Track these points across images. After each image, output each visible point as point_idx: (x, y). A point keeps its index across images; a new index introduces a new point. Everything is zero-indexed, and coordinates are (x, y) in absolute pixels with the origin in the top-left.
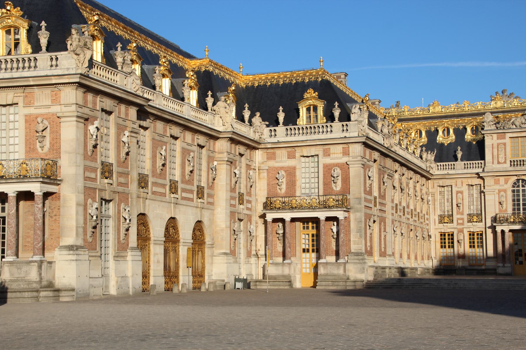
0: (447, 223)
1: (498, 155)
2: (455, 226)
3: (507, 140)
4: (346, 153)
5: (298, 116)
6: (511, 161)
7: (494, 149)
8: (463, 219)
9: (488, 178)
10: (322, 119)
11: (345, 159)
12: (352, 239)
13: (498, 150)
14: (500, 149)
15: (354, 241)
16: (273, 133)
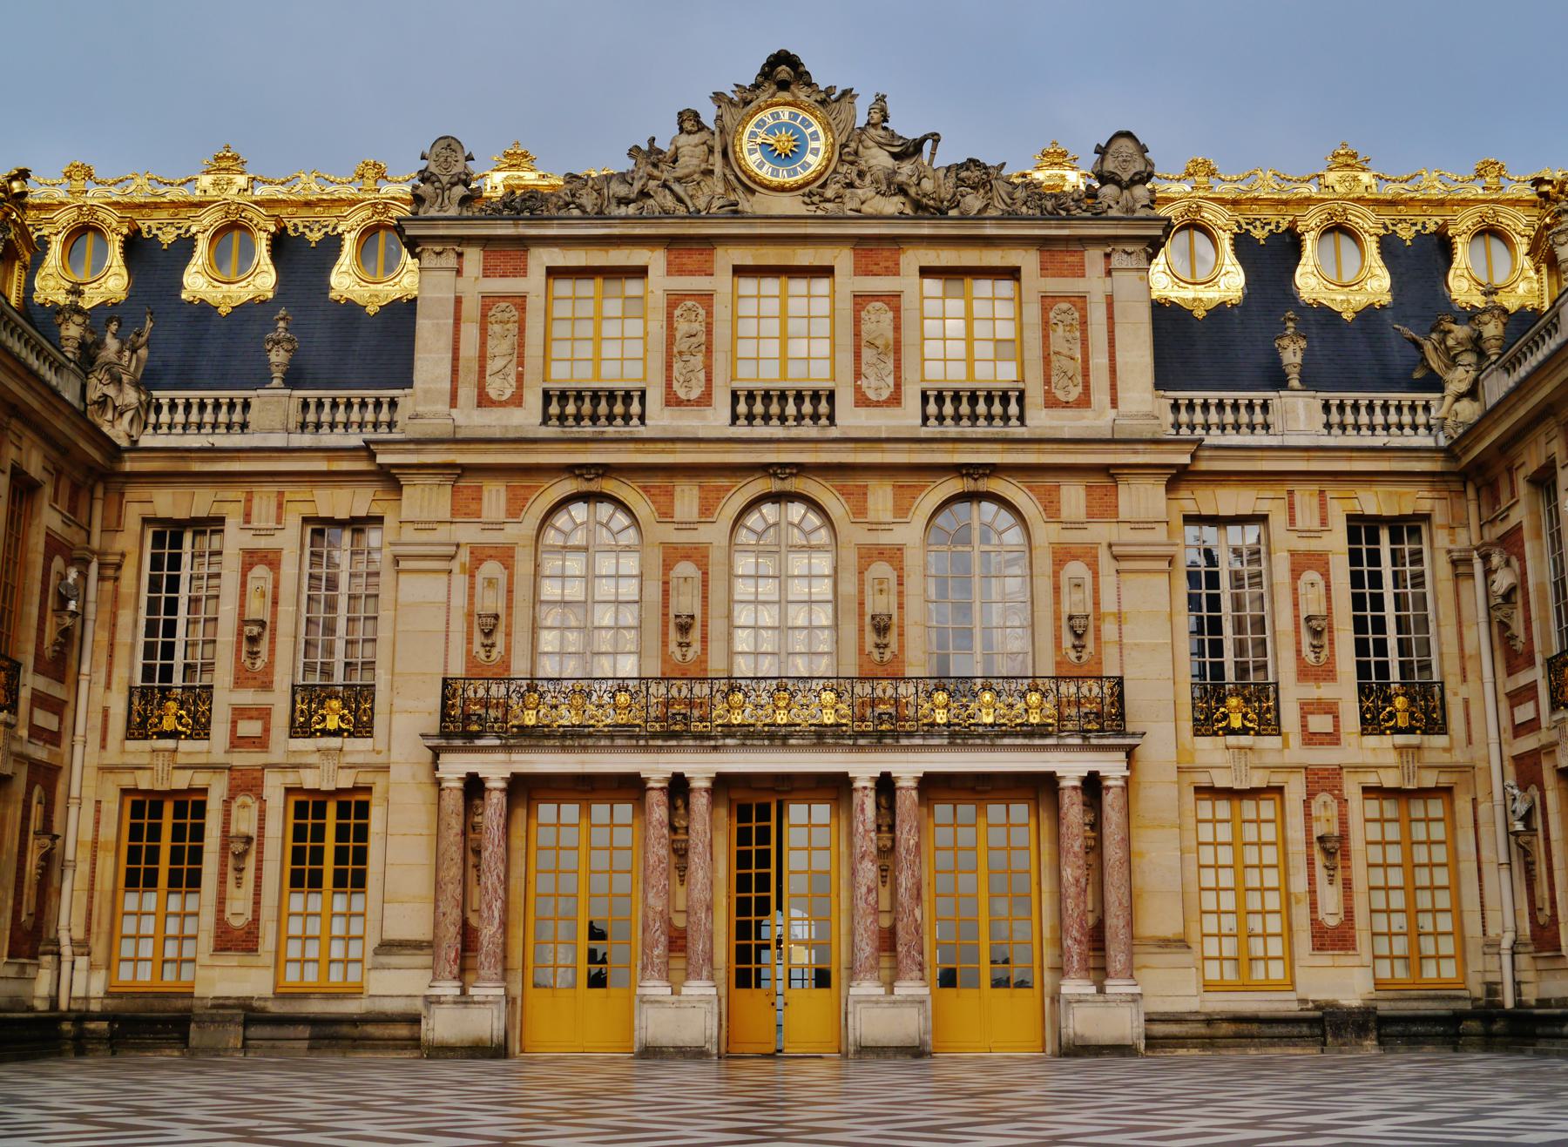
0: (174, 735)
1: (483, 358)
3: (533, 282)
6: (547, 397)
7: (464, 327)
8: (264, 714)
9: (418, 480)
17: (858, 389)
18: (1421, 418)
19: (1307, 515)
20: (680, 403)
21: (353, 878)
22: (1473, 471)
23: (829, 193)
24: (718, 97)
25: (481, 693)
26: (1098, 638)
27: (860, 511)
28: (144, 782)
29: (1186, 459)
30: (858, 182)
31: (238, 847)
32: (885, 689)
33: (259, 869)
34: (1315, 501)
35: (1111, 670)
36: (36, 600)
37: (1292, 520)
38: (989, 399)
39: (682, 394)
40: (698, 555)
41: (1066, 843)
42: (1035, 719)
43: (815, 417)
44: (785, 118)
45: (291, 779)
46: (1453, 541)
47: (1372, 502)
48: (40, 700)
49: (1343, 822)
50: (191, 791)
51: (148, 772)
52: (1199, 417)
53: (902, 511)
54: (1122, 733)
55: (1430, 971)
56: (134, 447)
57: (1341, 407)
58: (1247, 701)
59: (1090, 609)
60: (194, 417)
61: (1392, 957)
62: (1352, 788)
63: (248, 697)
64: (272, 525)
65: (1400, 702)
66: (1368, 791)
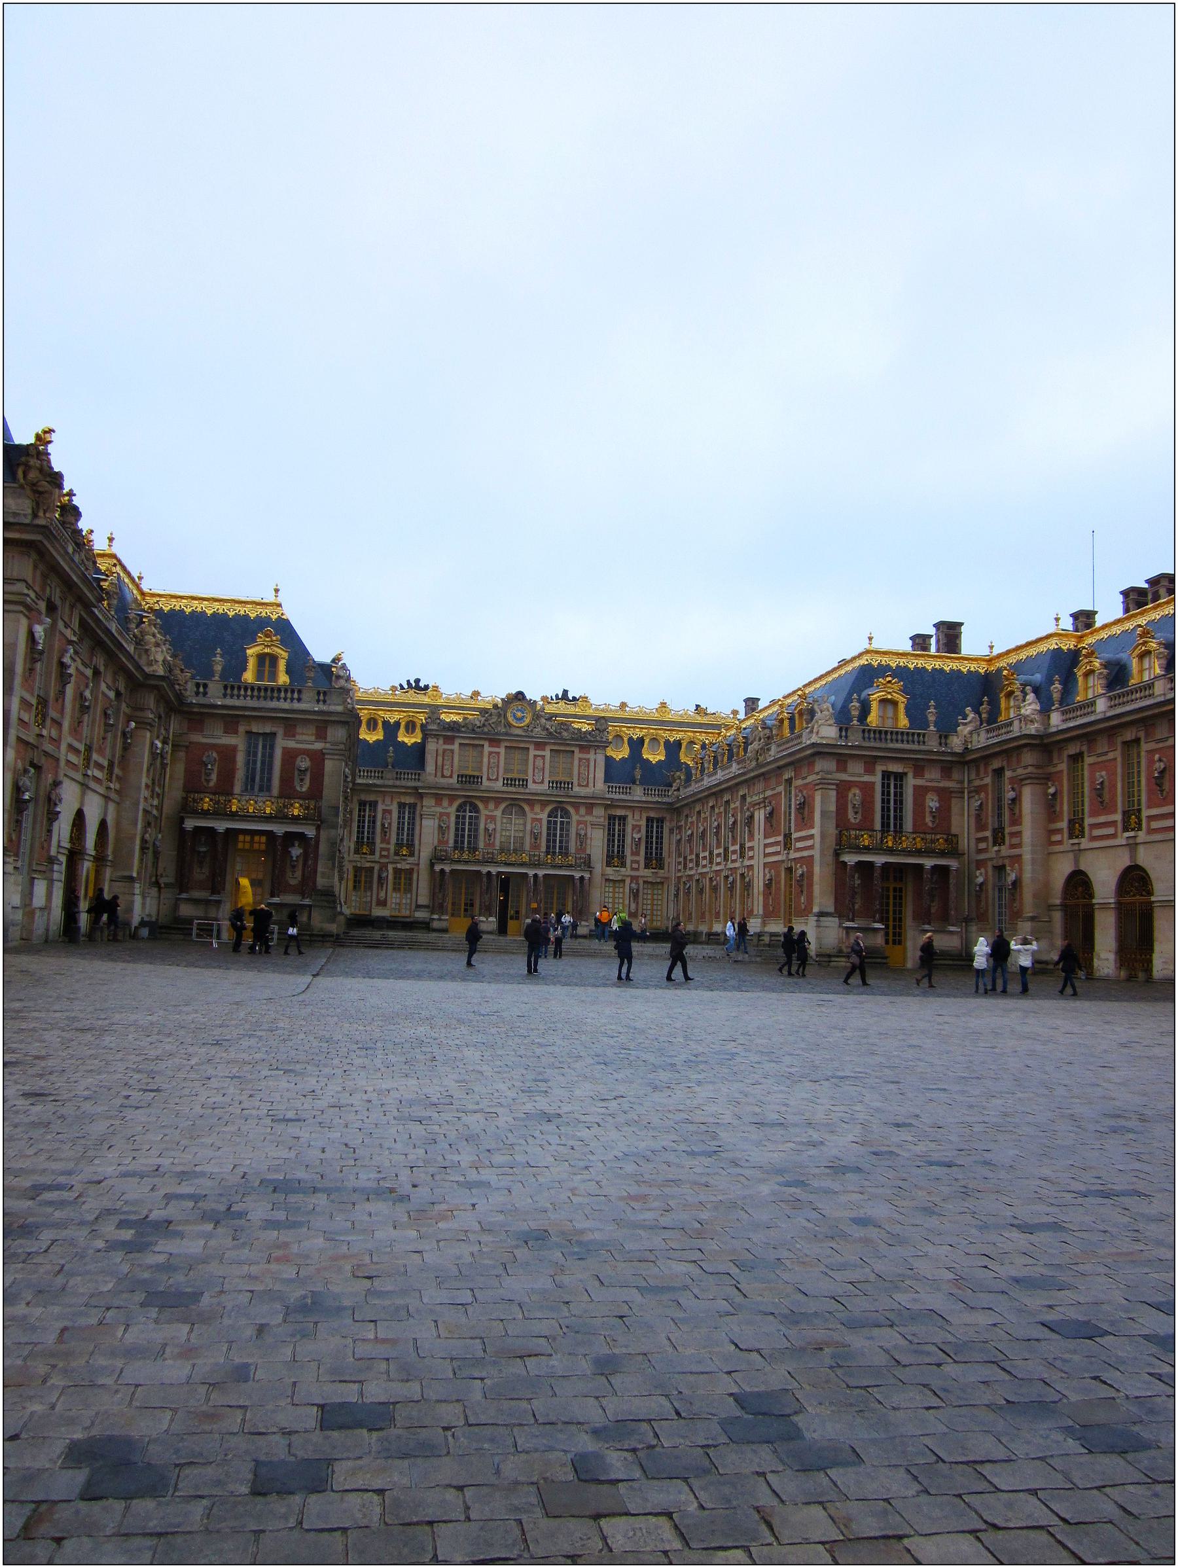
3: (456, 747)
4: (321, 735)
5: (245, 669)
10: (283, 679)
11: (318, 746)
12: (320, 869)
15: (323, 873)
16: (201, 689)
19: (637, 817)
21: (408, 890)
22: (675, 809)
27: (532, 809)
40: (492, 818)
47: (652, 814)
53: (542, 810)
62: (641, 882)
63: (384, 846)
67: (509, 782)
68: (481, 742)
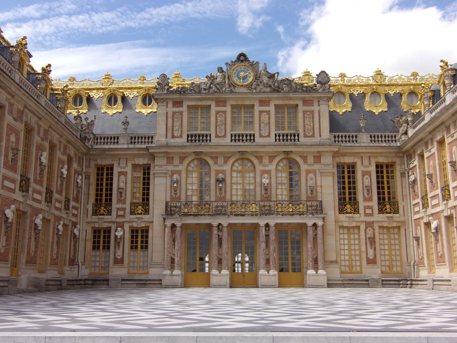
0: (103, 214)
2: (114, 219)
3: (184, 109)
6: (188, 136)
7: (168, 119)
8: (124, 209)
9: (159, 155)
13: (173, 120)
14: (176, 120)
17: (260, 133)
18: (394, 139)
19: (366, 162)
20: (219, 137)
21: (145, 247)
23: (253, 87)
24: (227, 64)
25: (175, 205)
26: (316, 191)
27: (261, 162)
28: (96, 226)
29: (337, 150)
30: (260, 84)
31: (118, 240)
32: (267, 203)
33: (123, 245)
34: (368, 159)
35: (319, 199)
36: (73, 184)
37: (362, 164)
38: (291, 136)
39: (219, 135)
40: (223, 172)
41: (308, 239)
42: (301, 210)
43: (250, 140)
44: (243, 69)
45: (130, 224)
46: (401, 168)
47: (382, 160)
48: (74, 208)
49: (374, 234)
50: (108, 227)
51: (97, 224)
52: (340, 139)
53: (271, 162)
54: (322, 213)
55: (394, 269)
56: (92, 148)
57: (374, 137)
58: (351, 206)
59: (314, 184)
60: (106, 140)
61: (385, 266)
62: (376, 226)
63: (120, 206)
64: (125, 166)
65: (388, 206)
66: (380, 227)
67: (236, 138)
68: (209, 103)
